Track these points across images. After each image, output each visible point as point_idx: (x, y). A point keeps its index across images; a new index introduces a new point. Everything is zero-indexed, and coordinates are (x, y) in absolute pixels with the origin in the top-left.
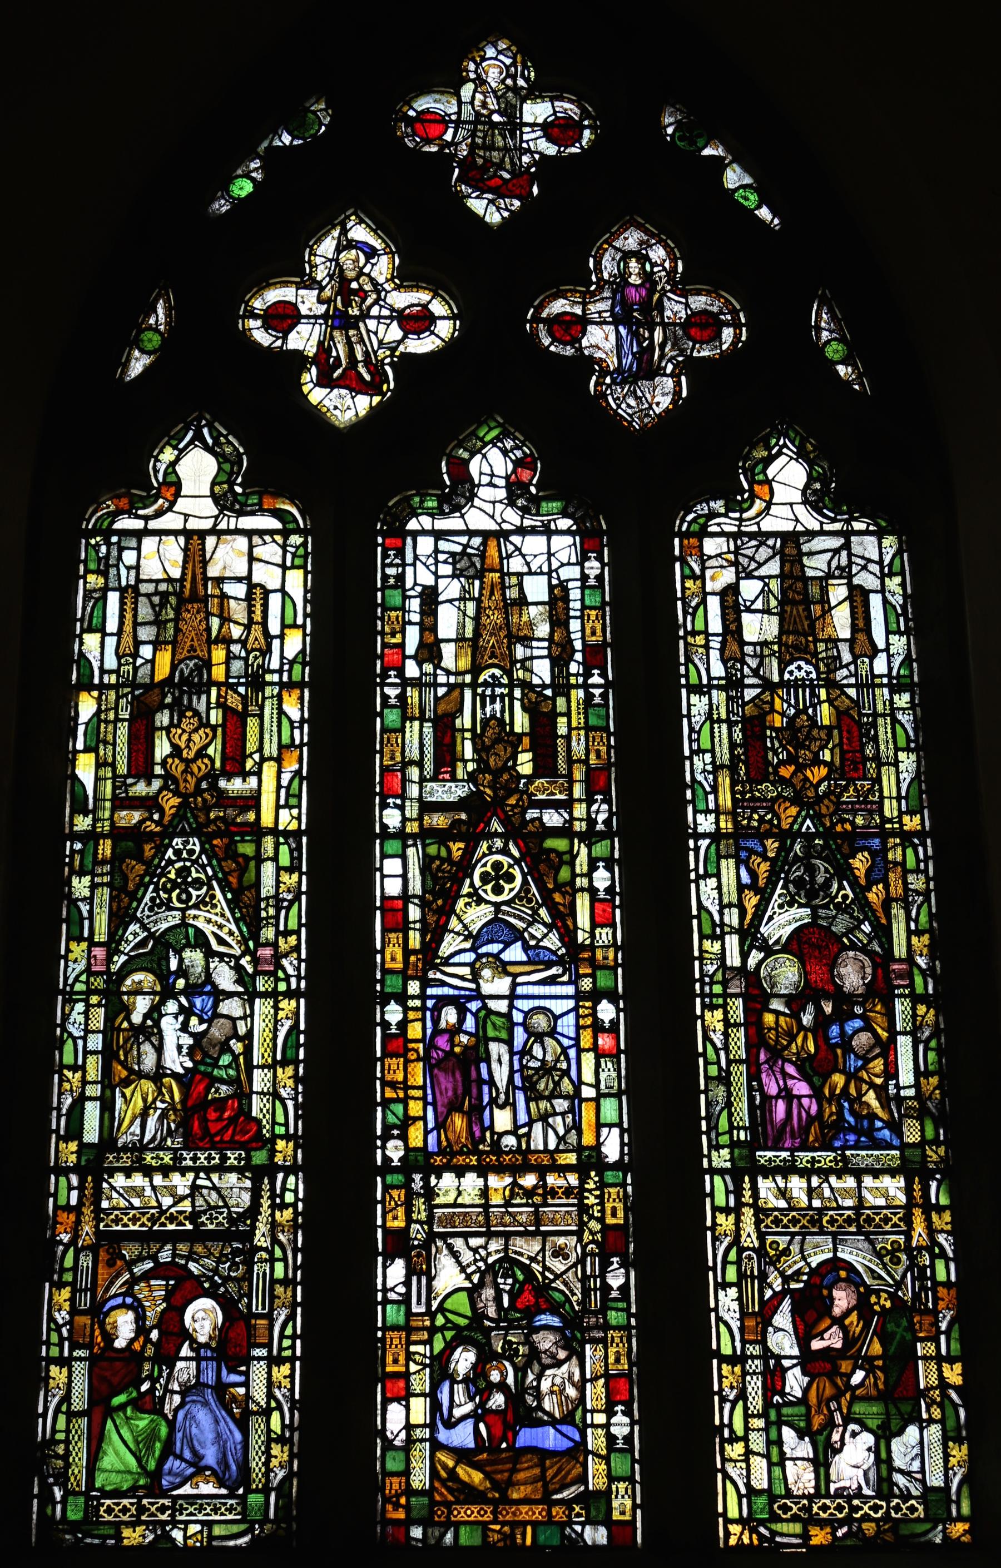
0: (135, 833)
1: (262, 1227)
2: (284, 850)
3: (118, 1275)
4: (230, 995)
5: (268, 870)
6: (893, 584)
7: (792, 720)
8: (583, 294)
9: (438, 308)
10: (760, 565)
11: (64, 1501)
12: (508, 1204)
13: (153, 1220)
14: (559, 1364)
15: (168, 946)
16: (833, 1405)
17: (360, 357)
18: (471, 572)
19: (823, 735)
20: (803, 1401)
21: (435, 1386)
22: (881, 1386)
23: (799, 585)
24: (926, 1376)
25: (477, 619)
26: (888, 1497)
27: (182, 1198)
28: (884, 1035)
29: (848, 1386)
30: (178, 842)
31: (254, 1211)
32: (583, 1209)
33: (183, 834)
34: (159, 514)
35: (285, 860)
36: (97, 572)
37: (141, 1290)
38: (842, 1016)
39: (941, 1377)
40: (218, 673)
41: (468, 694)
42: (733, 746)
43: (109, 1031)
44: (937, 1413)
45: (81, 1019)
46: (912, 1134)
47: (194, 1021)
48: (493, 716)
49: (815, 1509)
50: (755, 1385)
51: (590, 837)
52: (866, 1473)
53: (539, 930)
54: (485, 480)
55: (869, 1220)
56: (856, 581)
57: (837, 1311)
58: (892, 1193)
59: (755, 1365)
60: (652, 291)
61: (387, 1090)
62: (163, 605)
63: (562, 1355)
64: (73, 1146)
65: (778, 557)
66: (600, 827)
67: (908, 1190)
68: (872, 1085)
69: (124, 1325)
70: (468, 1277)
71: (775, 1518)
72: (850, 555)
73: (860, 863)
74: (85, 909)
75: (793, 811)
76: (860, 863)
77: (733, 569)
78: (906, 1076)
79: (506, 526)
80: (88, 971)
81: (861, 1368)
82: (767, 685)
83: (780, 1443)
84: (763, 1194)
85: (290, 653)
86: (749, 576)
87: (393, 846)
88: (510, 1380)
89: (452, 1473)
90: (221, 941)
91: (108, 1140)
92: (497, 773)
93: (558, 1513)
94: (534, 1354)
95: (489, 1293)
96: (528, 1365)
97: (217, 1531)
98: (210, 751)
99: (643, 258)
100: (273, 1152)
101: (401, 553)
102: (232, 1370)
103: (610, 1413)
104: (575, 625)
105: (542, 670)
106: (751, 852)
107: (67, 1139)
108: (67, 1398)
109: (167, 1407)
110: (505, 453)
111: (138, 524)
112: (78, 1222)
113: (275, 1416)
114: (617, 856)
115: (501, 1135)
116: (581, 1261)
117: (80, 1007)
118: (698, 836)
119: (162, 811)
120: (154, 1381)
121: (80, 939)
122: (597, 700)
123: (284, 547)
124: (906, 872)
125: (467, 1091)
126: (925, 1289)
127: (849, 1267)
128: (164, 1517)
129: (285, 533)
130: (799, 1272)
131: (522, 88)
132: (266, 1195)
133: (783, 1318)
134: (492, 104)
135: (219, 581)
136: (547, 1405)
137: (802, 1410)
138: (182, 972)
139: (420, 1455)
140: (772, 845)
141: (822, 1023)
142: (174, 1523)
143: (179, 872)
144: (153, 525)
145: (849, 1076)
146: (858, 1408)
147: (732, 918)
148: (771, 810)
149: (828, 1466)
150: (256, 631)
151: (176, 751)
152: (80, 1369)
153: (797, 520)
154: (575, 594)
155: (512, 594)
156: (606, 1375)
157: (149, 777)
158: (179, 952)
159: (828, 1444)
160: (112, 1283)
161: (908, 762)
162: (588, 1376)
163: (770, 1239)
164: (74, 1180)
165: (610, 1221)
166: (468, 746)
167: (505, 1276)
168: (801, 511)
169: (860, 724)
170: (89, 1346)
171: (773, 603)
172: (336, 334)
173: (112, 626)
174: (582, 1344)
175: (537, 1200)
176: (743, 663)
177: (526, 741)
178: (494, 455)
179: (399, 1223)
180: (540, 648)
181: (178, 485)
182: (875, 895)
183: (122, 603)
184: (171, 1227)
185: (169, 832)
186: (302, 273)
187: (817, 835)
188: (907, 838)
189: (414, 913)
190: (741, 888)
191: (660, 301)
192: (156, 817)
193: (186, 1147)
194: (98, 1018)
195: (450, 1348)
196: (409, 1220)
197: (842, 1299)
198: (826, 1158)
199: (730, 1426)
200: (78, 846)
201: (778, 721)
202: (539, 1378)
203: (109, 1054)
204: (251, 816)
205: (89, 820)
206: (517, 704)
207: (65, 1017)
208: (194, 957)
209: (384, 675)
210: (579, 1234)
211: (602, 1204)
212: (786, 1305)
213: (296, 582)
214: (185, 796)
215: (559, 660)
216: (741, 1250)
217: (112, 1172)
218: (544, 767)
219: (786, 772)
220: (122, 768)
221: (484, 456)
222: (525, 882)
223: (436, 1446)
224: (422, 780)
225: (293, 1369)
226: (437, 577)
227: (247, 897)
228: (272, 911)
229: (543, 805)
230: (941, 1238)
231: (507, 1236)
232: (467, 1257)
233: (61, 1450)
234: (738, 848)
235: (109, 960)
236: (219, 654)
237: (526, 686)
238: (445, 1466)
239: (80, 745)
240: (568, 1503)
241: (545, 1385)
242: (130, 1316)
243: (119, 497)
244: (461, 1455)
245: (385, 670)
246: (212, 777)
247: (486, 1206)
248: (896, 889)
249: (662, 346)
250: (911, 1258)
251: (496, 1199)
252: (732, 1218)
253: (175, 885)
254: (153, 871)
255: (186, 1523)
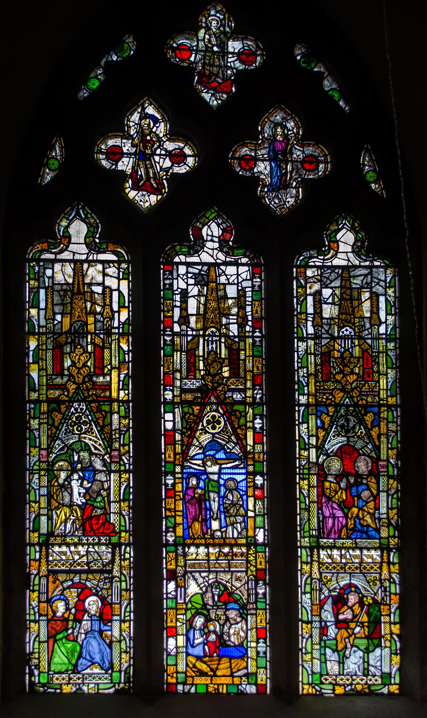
0: (57, 401)
1: (116, 568)
2: (122, 408)
3: (57, 587)
4: (101, 471)
5: (115, 417)
6: (390, 292)
7: (342, 354)
8: (256, 145)
9: (187, 151)
10: (331, 282)
11: (39, 675)
12: (217, 559)
13: (71, 565)
14: (237, 623)
15: (73, 450)
16: (347, 640)
17: (151, 175)
18: (203, 283)
19: (356, 361)
20: (335, 639)
21: (188, 631)
22: (366, 633)
23: (349, 291)
24: (385, 629)
25: (205, 305)
26: (367, 676)
27: (83, 556)
28: (375, 492)
29: (353, 633)
30: (76, 405)
31: (113, 561)
32: (248, 562)
33: (78, 401)
34: (61, 252)
35: (122, 413)
36: (34, 279)
37: (67, 593)
38: (357, 484)
39: (391, 630)
40: (91, 328)
41: (201, 340)
42: (316, 365)
43: (49, 486)
44: (388, 644)
45: (37, 481)
46: (384, 533)
47: (85, 482)
48: (212, 350)
49: (338, 680)
50: (316, 633)
51: (253, 404)
52: (359, 667)
53: (230, 445)
54: (209, 238)
55: (365, 568)
56: (374, 290)
57: (350, 604)
58: (375, 557)
59: (317, 625)
60: (287, 144)
61: (167, 512)
62: (65, 296)
63: (239, 619)
64: (36, 535)
65: (339, 278)
66: (258, 400)
67: (382, 556)
68: (369, 513)
69: (61, 607)
70: (201, 589)
71: (322, 683)
72: (372, 277)
73: (369, 418)
74: (37, 434)
75: (341, 394)
76: (369, 418)
77: (319, 283)
78: (383, 510)
79: (218, 261)
80: (39, 460)
81: (359, 626)
82: (333, 338)
83: (325, 654)
84: (322, 556)
85: (123, 319)
86: (327, 287)
87: (168, 408)
88: (218, 629)
89: (194, 666)
90: (96, 448)
91: (50, 534)
92: (214, 376)
93: (237, 681)
94: (227, 619)
95: (209, 595)
96: (225, 623)
97: (101, 686)
98: (89, 364)
99: (284, 127)
100: (120, 537)
101: (171, 273)
102: (105, 625)
103: (257, 642)
104: (249, 309)
105: (234, 329)
106: (322, 412)
107: (34, 531)
108: (38, 636)
109: (79, 639)
110: (218, 225)
111: (52, 256)
112: (40, 566)
113: (123, 642)
114: (265, 413)
115: (215, 531)
116: (247, 583)
117: (36, 476)
118: (300, 405)
119: (68, 391)
120: (74, 629)
121: (35, 447)
122: (258, 343)
123: (118, 269)
124: (388, 422)
125: (201, 513)
126: (386, 595)
127: (356, 587)
128: (80, 681)
129: (119, 262)
130: (335, 588)
131: (228, 32)
132: (117, 555)
133: (328, 606)
134: (213, 40)
135: (90, 284)
136: (232, 639)
137: (334, 642)
138: (80, 461)
139: (182, 657)
140: (331, 409)
141: (349, 486)
142: (84, 684)
143: (77, 418)
144: (59, 257)
145: (360, 509)
146: (357, 641)
147: (313, 441)
148: (331, 394)
149: (343, 663)
150: (107, 309)
151: (74, 364)
152: (43, 624)
153: (349, 260)
154: (249, 294)
155: (221, 293)
156: (257, 628)
157: (62, 375)
158: (78, 453)
159: (344, 655)
160: (55, 590)
161: (391, 374)
162: (249, 628)
163: (324, 575)
164: (38, 549)
165: (259, 567)
166: (201, 363)
167: (216, 588)
168: (351, 255)
169: (372, 356)
170: (47, 615)
171: (336, 300)
172: (141, 163)
173: (42, 305)
174: (247, 615)
175: (230, 558)
176: (322, 327)
177: (226, 361)
178: (214, 226)
179: (173, 567)
180: (233, 319)
181: (69, 237)
183: (46, 295)
184: (79, 568)
185: (71, 401)
186: (123, 131)
187: (351, 405)
188: (389, 407)
189: (178, 437)
190: (317, 428)
191: (291, 149)
192: (66, 393)
193: (84, 535)
194: (45, 481)
195: (194, 616)
196: (177, 566)
197: (352, 599)
198: (349, 543)
199: (306, 648)
200: (32, 406)
201: (337, 354)
202: (229, 628)
203: (50, 496)
204: (108, 394)
205: (36, 395)
206: (223, 345)
207: (30, 481)
209: (164, 331)
210: (246, 572)
211: (256, 560)
212: (330, 601)
213: (124, 286)
214: (78, 384)
215: (241, 326)
216: (312, 579)
217: (53, 545)
218: (234, 374)
219: (339, 377)
220: (50, 371)
221: (209, 227)
222: (225, 424)
223: (188, 654)
224: (181, 379)
225: (130, 625)
226: (188, 285)
227: (107, 429)
228: (117, 436)
229: (234, 391)
230: (394, 576)
231: (217, 572)
232: (200, 580)
233: (37, 656)
234: (317, 411)
235: (48, 456)
236: (91, 320)
237: (227, 336)
238: (191, 662)
239: (31, 361)
240: (241, 677)
241: (232, 631)
242: (63, 603)
243: (43, 243)
244: (198, 658)
245: (165, 328)
246: (90, 376)
247: (208, 560)
248: (383, 430)
249: (291, 172)
250: (381, 583)
251: (212, 557)
252: (309, 566)
253: (75, 424)
254: (66, 418)
255: (88, 684)
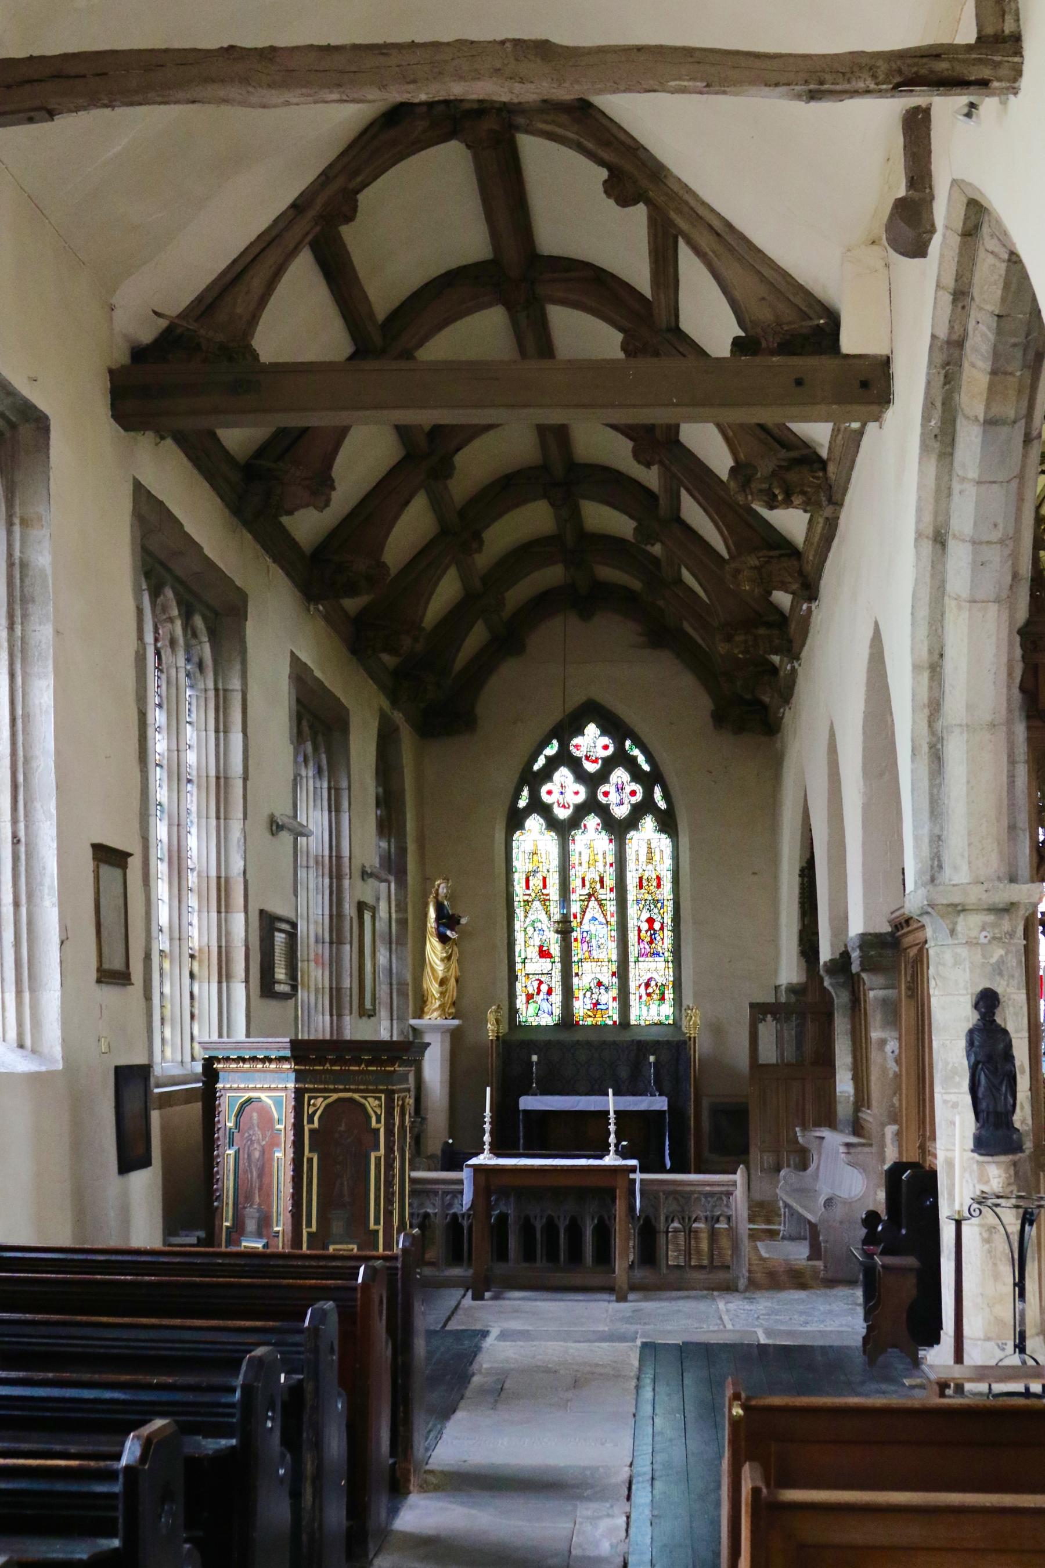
0: (527, 901)
24: (666, 997)
38: (654, 934)
46: (666, 954)
50: (638, 998)
73: (659, 905)
76: (659, 905)
91: (526, 958)
133: (643, 986)
140: (643, 902)
141: (651, 935)
182: (662, 911)
197: (653, 983)
208: (539, 924)
218: (602, 887)
